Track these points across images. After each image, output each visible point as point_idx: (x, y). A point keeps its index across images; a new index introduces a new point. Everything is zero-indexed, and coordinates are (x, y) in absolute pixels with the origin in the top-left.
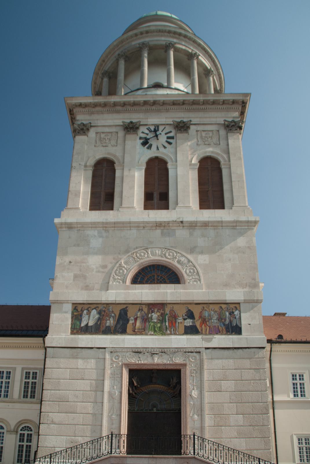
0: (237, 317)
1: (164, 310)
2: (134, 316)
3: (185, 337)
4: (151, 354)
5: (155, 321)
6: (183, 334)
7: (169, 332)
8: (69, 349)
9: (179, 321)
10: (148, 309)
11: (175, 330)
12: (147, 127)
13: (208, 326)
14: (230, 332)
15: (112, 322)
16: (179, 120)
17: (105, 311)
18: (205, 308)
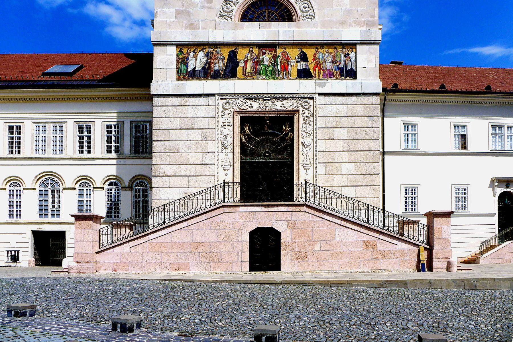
0: (353, 60)
2: (244, 59)
3: (298, 81)
4: (263, 100)
5: (267, 64)
7: (281, 76)
9: (292, 64)
11: (287, 74)
13: (321, 68)
15: (221, 64)
17: (213, 53)
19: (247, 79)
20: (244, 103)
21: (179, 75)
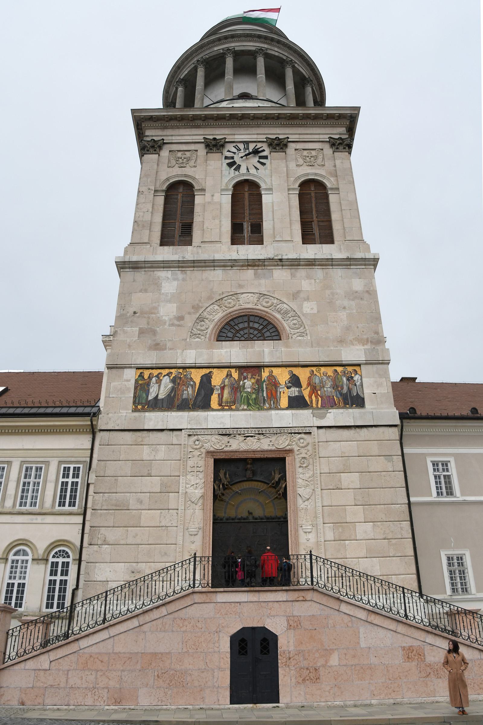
0: (358, 384)
1: (260, 375)
2: (221, 385)
3: (289, 412)
4: (245, 437)
5: (249, 390)
6: (287, 409)
7: (267, 405)
8: (131, 433)
10: (239, 375)
11: (276, 402)
12: (234, 144)
14: (349, 405)
15: (190, 392)
16: (274, 137)
17: (180, 378)
18: (315, 372)
19: (223, 410)
20: (219, 441)
21: (137, 405)
